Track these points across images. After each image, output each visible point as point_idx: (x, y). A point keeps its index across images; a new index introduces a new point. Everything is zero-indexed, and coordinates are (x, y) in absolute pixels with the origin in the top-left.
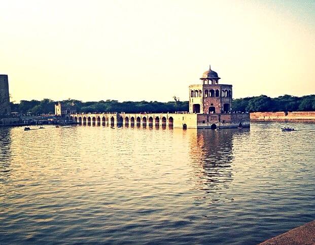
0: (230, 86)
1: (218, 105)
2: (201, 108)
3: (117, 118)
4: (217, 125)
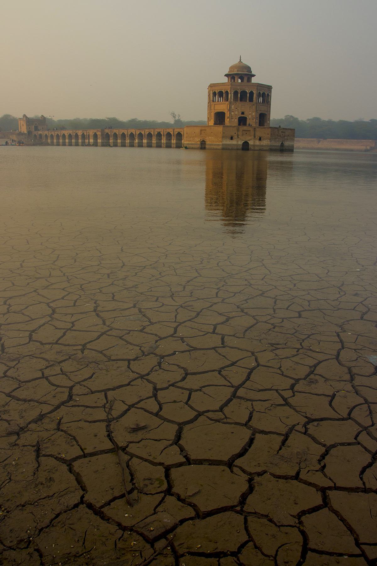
0: (270, 88)
1: (252, 115)
2: (226, 118)
3: (102, 135)
4: (251, 143)
